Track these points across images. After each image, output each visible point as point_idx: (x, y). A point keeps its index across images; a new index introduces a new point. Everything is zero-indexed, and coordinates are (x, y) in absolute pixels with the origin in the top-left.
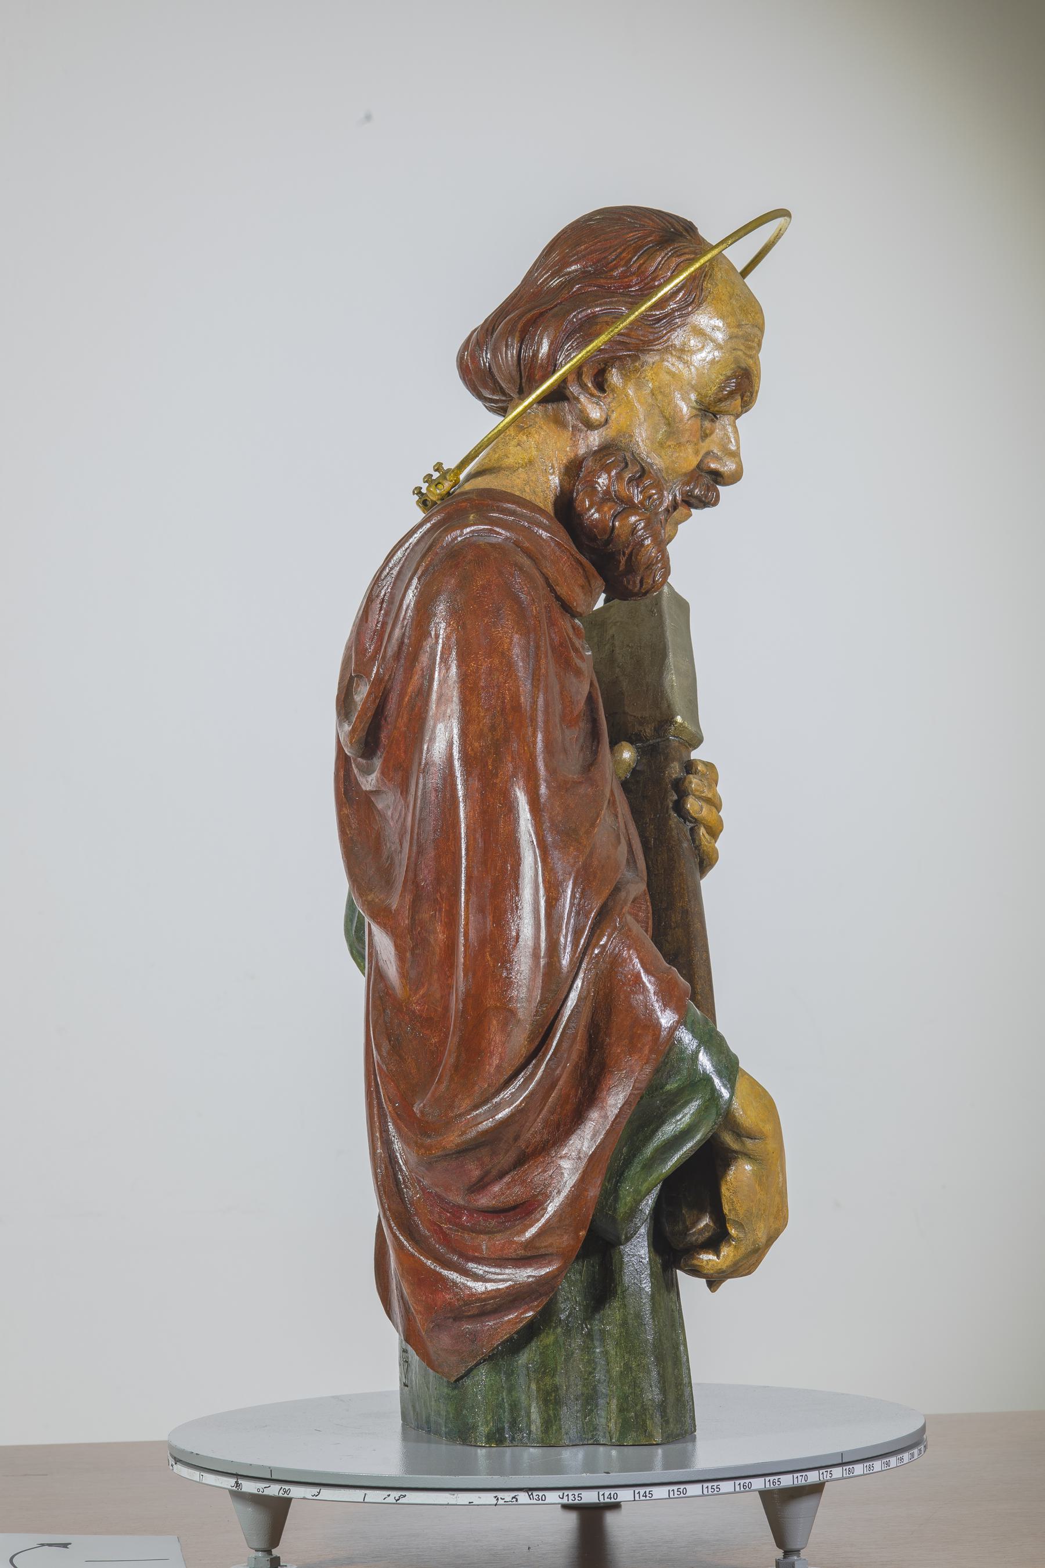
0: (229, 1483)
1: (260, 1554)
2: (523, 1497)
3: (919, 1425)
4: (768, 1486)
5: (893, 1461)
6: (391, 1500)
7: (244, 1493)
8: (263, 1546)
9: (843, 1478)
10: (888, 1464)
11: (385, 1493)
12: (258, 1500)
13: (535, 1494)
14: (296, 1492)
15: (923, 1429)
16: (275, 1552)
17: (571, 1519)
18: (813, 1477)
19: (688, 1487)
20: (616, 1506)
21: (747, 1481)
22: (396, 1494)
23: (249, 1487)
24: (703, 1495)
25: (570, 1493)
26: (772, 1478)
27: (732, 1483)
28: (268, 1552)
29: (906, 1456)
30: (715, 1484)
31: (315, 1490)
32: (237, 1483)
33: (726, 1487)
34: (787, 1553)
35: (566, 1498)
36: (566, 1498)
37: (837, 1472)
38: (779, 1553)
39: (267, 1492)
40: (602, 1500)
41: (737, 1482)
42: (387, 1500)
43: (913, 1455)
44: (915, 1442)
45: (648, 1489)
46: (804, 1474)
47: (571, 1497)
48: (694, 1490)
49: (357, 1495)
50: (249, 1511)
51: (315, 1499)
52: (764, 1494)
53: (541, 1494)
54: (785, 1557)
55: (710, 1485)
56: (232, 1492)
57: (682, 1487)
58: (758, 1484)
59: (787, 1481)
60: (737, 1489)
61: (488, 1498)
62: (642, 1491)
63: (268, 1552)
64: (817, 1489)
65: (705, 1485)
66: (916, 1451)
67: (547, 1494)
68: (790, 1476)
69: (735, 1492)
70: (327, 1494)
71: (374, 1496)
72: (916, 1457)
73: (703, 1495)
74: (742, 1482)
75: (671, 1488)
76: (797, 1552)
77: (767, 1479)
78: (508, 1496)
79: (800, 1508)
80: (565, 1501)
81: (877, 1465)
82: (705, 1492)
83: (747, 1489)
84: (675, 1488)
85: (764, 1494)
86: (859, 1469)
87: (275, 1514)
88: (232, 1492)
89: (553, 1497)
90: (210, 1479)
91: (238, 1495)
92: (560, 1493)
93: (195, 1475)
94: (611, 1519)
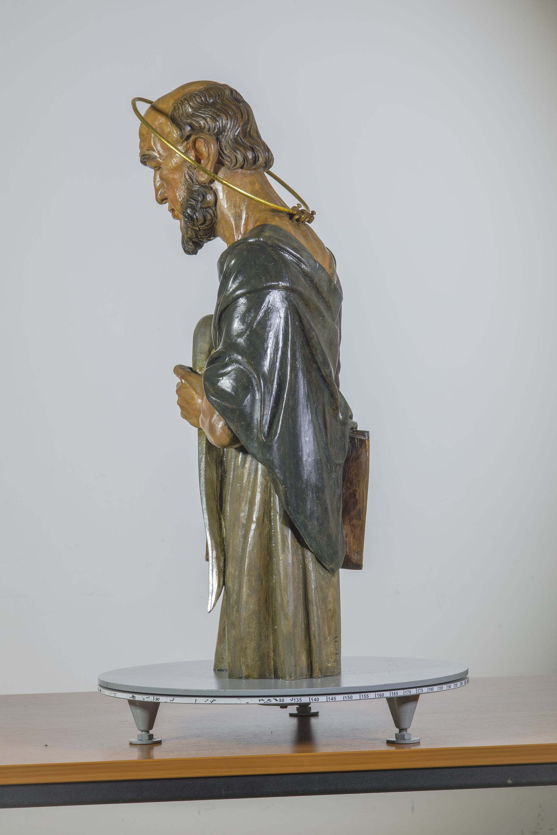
1: (144, 733)
5: (452, 685)
7: (136, 701)
9: (428, 693)
10: (450, 687)
12: (143, 705)
16: (151, 732)
18: (413, 692)
26: (393, 692)
28: (148, 732)
29: (459, 684)
34: (401, 730)
37: (425, 690)
38: (397, 731)
39: (146, 700)
50: (139, 711)
54: (400, 732)
59: (401, 693)
64: (415, 698)
66: (463, 682)
68: (402, 691)
72: (463, 684)
76: (405, 730)
79: (408, 707)
81: (445, 687)
85: (390, 700)
86: (436, 688)
90: (119, 695)
91: (132, 703)
93: (111, 693)
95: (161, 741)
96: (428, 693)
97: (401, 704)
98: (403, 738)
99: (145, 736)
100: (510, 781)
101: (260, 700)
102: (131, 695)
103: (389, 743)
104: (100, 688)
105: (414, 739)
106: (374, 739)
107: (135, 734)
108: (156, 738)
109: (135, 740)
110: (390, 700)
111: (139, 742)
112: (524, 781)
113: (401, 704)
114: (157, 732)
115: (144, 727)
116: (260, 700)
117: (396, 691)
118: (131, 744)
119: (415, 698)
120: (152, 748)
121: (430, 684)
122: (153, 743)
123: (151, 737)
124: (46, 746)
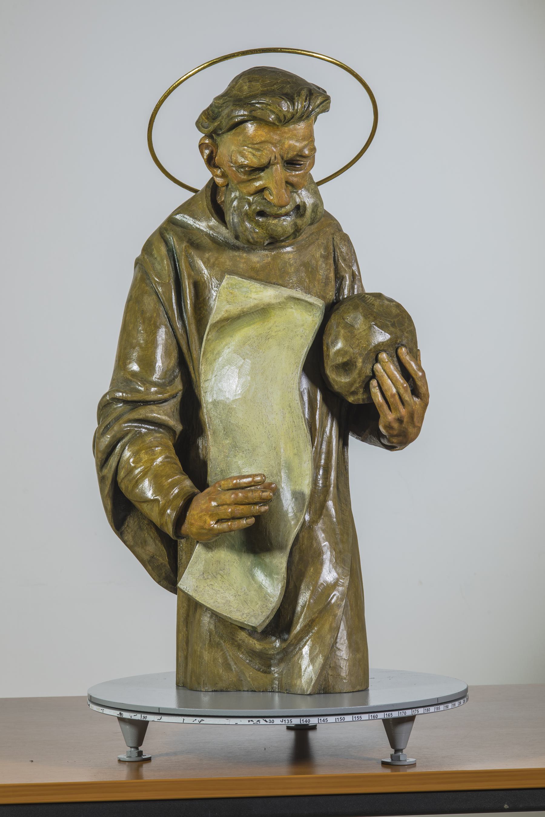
0: (116, 713)
1: (133, 749)
2: (262, 721)
3: (464, 688)
4: (386, 717)
5: (450, 706)
6: (197, 722)
8: (134, 746)
9: (424, 713)
10: (447, 707)
11: (195, 718)
13: (268, 720)
14: (150, 718)
15: (466, 691)
16: (140, 748)
17: (292, 735)
18: (409, 713)
19: (346, 717)
20: (314, 728)
21: (375, 714)
22: (199, 719)
23: (126, 715)
24: (353, 721)
25: (286, 719)
27: (367, 715)
28: (137, 748)
29: (457, 703)
30: (359, 715)
31: (159, 717)
32: (120, 713)
33: (365, 717)
34: (397, 751)
35: (284, 722)
36: (284, 722)
37: (421, 710)
38: (392, 751)
40: (302, 723)
41: (370, 715)
42: (195, 722)
43: (460, 703)
44: (462, 696)
45: (325, 718)
46: (404, 711)
47: (287, 721)
48: (348, 718)
49: (180, 719)
50: (127, 727)
51: (159, 721)
52: (386, 721)
53: (271, 719)
54: (395, 753)
55: (356, 716)
56: (118, 718)
57: (342, 717)
58: (381, 716)
59: (395, 714)
60: (370, 718)
61: (245, 721)
62: (322, 718)
63: (137, 748)
64: (411, 719)
65: (354, 716)
67: (275, 720)
69: (369, 720)
70: (165, 719)
71: (188, 720)
72: (462, 704)
73: (353, 721)
74: (373, 714)
75: (337, 717)
76: (401, 750)
77: (386, 713)
78: (255, 720)
80: (284, 723)
81: (442, 707)
82: (354, 719)
83: (375, 718)
84: (339, 717)
85: (385, 721)
86: (432, 709)
87: (140, 729)
88: (118, 718)
89: (277, 721)
90: (107, 711)
91: (121, 720)
92: (281, 719)
94: (312, 735)
95: (151, 757)
96: (424, 713)
97: (396, 725)
98: (398, 759)
99: (134, 753)
100: (506, 806)
101: (249, 721)
102: (118, 712)
103: (384, 764)
104: (89, 703)
105: (411, 760)
106: (369, 759)
107: (124, 751)
108: (146, 755)
109: (123, 757)
110: (385, 721)
111: (128, 759)
112: (521, 806)
113: (396, 725)
114: (147, 748)
115: (132, 743)
116: (249, 721)
117: (390, 713)
118: (120, 761)
119: (411, 719)
120: (141, 766)
121: (426, 705)
122: (141, 761)
123: (140, 753)
124: (32, 761)
